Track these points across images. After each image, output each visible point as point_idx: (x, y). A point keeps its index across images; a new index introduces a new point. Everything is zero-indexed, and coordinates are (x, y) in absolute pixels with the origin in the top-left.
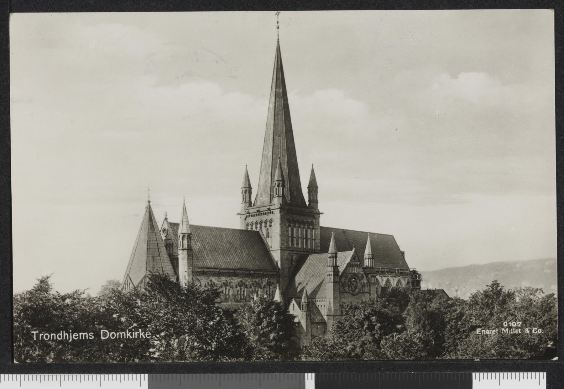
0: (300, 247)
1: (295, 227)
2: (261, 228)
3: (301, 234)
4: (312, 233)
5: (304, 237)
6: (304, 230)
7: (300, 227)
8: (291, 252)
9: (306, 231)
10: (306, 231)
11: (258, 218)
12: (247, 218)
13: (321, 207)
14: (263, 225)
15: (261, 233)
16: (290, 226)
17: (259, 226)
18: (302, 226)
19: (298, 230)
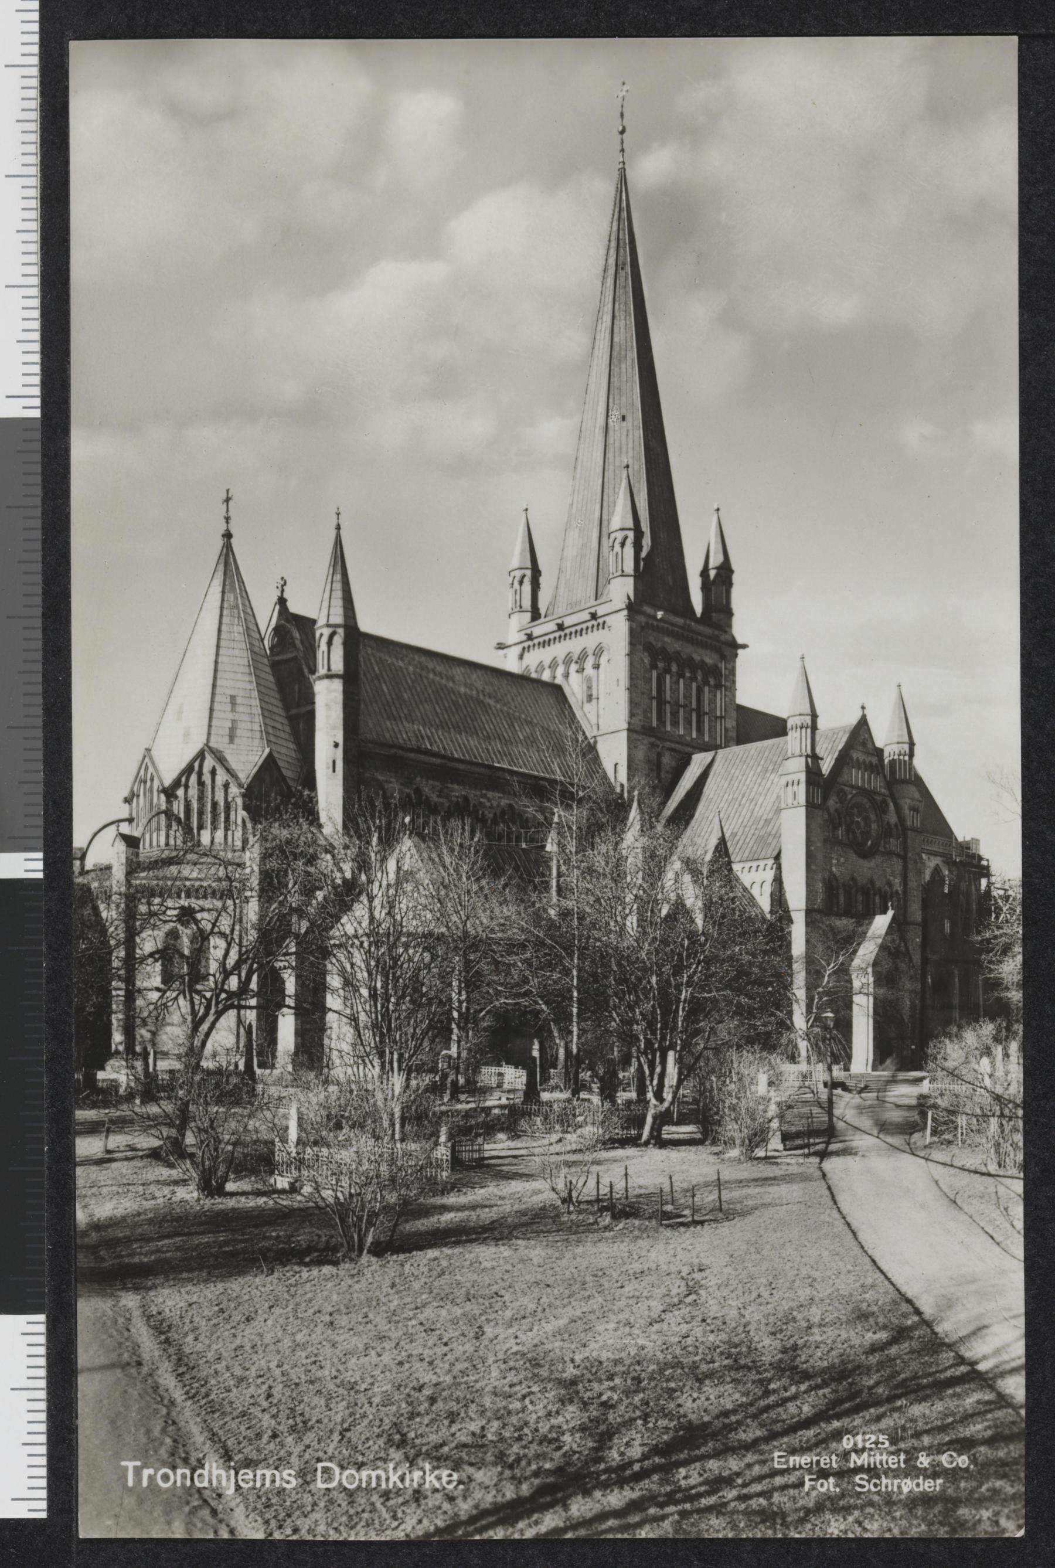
0: (681, 732)
1: (668, 671)
2: (567, 675)
3: (685, 697)
4: (715, 700)
5: (694, 706)
6: (694, 685)
7: (681, 675)
8: (658, 742)
9: (700, 691)
10: (700, 691)
11: (559, 650)
12: (526, 655)
13: (741, 629)
14: (574, 667)
15: (567, 691)
16: (654, 666)
17: (560, 670)
18: (688, 675)
19: (678, 683)
